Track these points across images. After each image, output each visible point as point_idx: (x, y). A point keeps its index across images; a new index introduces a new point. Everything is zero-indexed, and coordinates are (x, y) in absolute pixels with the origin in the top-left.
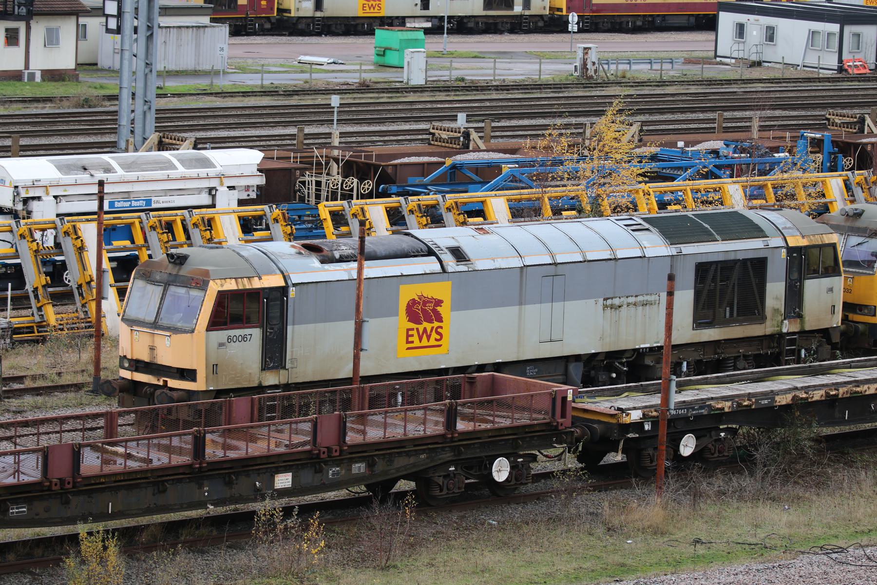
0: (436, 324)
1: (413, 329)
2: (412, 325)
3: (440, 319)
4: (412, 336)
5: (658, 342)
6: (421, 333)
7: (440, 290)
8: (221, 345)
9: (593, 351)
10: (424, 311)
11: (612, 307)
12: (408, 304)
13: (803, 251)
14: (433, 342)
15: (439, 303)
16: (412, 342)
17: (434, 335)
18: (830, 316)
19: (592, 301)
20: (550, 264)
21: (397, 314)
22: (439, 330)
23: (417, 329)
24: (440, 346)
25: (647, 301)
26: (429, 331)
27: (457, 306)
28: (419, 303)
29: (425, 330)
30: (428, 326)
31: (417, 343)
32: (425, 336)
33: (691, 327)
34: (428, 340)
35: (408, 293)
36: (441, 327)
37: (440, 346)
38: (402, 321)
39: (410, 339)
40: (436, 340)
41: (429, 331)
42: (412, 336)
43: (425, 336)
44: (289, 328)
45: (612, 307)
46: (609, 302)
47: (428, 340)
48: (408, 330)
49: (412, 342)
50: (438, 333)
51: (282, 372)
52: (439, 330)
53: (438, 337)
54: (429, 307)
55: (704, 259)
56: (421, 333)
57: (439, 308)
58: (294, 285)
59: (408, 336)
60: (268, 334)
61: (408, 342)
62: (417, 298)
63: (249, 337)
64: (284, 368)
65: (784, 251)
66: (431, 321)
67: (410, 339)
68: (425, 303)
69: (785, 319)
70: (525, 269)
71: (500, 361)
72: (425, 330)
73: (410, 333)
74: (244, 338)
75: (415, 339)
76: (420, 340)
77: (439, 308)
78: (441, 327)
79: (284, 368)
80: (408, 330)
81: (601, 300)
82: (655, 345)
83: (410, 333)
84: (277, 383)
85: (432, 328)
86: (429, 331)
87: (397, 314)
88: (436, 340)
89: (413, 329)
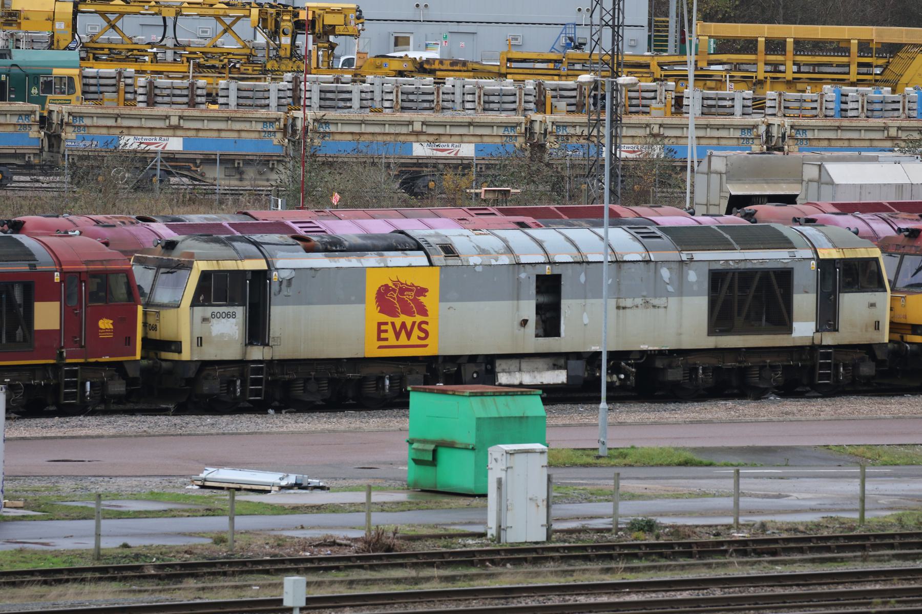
0: (419, 318)
1: (386, 324)
2: (384, 318)
3: (423, 311)
4: (386, 331)
6: (398, 330)
10: (400, 300)
12: (379, 292)
14: (414, 340)
15: (422, 291)
16: (386, 339)
17: (416, 332)
21: (362, 300)
22: (424, 326)
23: (393, 324)
24: (425, 346)
26: (409, 328)
27: (443, 298)
28: (394, 290)
29: (403, 325)
30: (409, 321)
31: (392, 341)
32: (403, 332)
34: (409, 338)
36: (426, 323)
37: (425, 346)
38: (371, 313)
39: (383, 335)
40: (419, 338)
41: (409, 328)
42: (386, 331)
43: (403, 332)
47: (409, 338)
48: (380, 324)
49: (386, 339)
52: (424, 326)
53: (423, 335)
54: (409, 296)
56: (398, 330)
57: (422, 299)
59: (380, 331)
61: (379, 339)
62: (391, 284)
65: (813, 264)
66: (410, 313)
67: (383, 335)
72: (403, 325)
73: (383, 327)
75: (391, 335)
77: (422, 299)
78: (426, 323)
80: (380, 324)
83: (383, 327)
85: (414, 323)
86: (409, 327)
88: (419, 338)
89: (386, 324)
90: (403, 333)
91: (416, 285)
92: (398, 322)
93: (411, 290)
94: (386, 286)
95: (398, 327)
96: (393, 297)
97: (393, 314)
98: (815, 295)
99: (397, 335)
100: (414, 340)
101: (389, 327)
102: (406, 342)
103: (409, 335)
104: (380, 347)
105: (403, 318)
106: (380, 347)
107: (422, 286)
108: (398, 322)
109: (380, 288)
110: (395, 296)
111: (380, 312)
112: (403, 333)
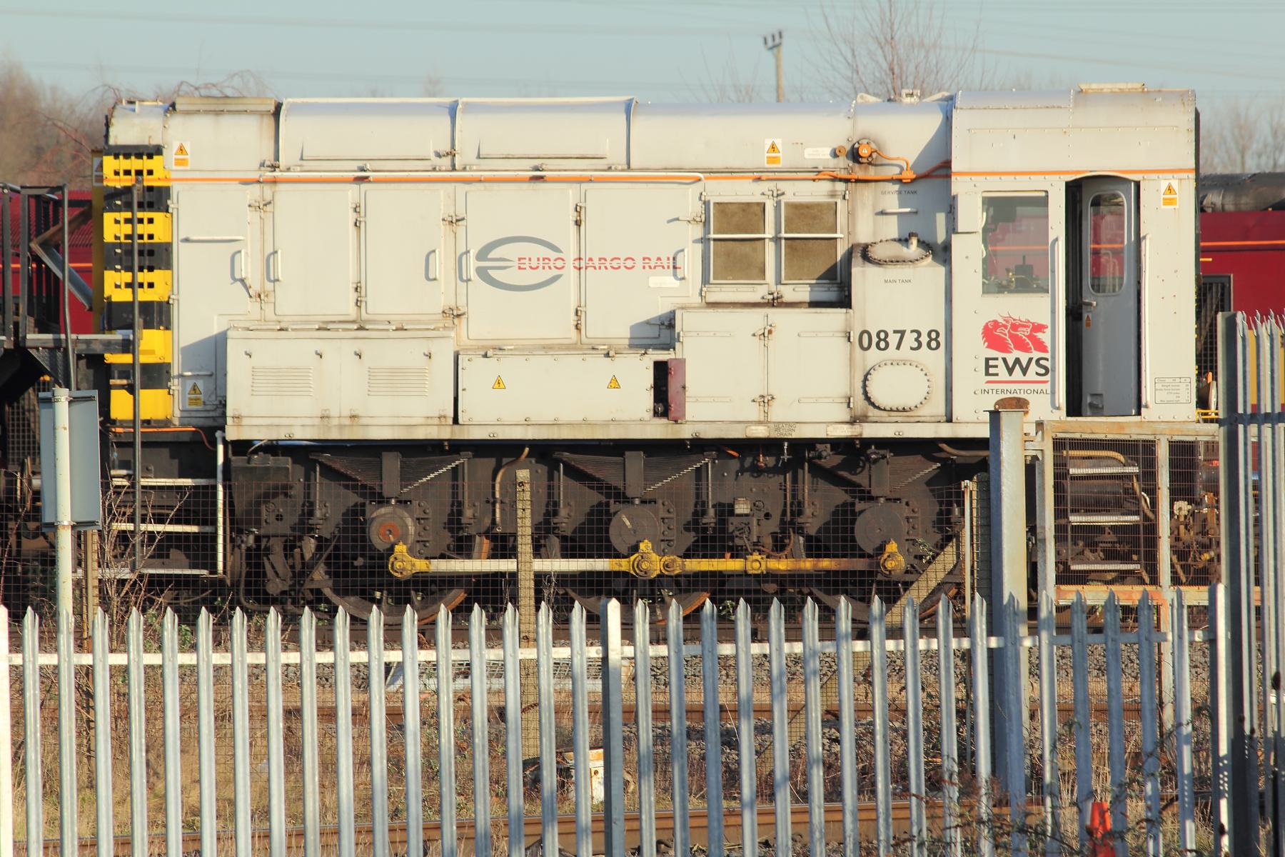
2: (993, 353)
23: (1005, 360)
28: (1006, 327)
29: (1017, 361)
30: (1024, 358)
39: (992, 370)
54: (1023, 333)
57: (1039, 335)
59: (987, 366)
61: (987, 374)
62: (1001, 320)
66: (1027, 350)
67: (992, 370)
68: (1015, 327)
72: (1017, 361)
73: (991, 363)
80: (987, 360)
83: (991, 363)
85: (1030, 360)
94: (996, 322)
96: (1004, 333)
97: (1004, 348)
99: (1010, 371)
102: (1022, 378)
103: (1024, 371)
104: (988, 382)
105: (1017, 354)
106: (988, 382)
107: (1039, 322)
110: (1006, 332)
111: (989, 347)
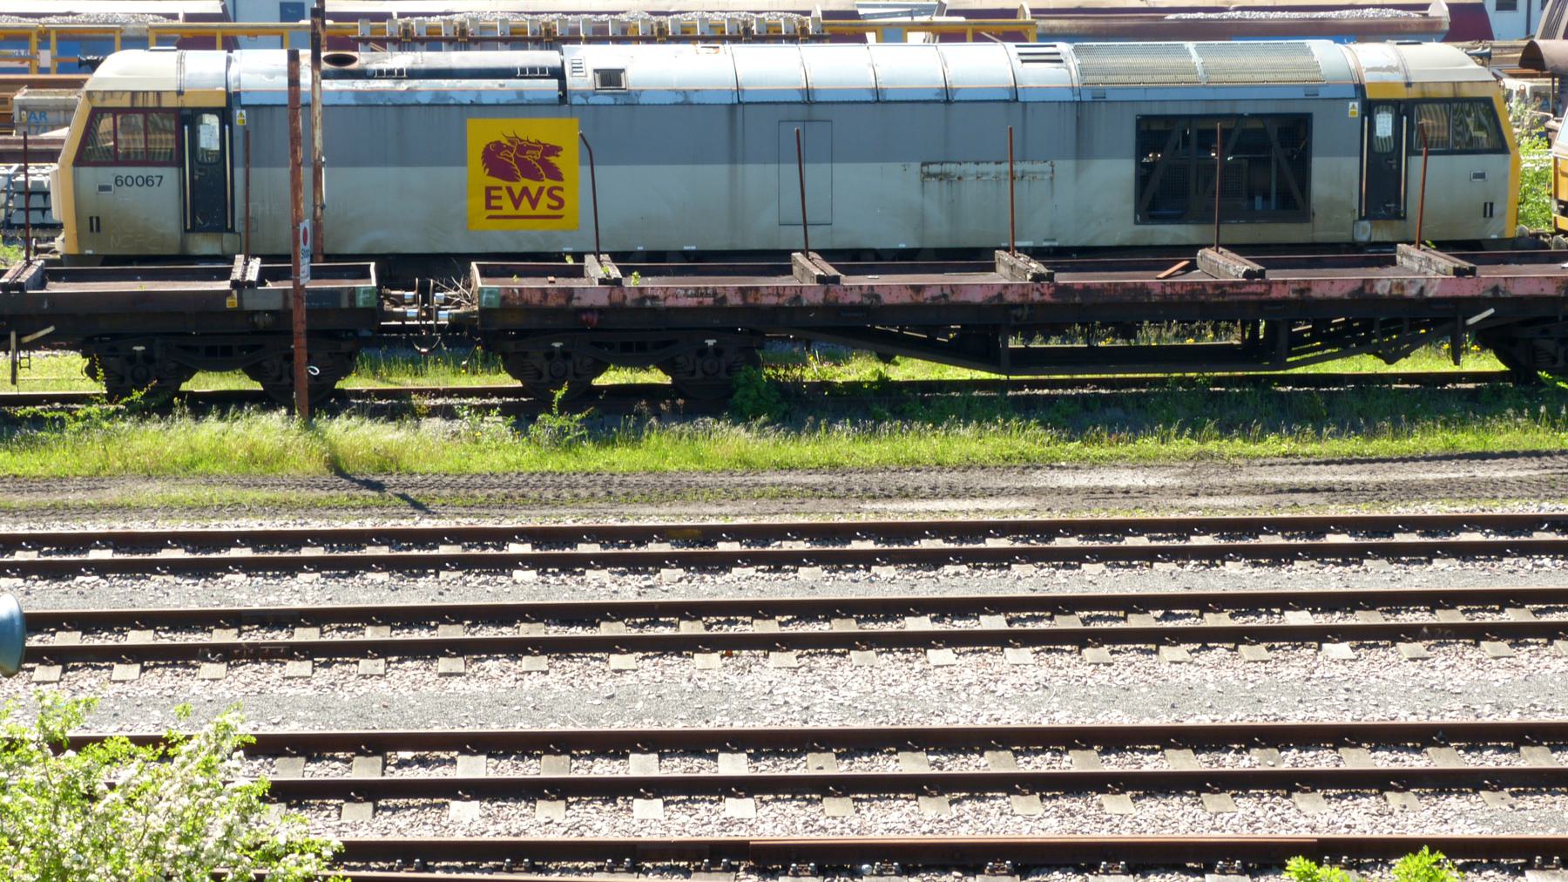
0: (548, 183)
1: (499, 188)
3: (555, 174)
4: (499, 198)
5: (1054, 240)
6: (517, 195)
7: (561, 132)
8: (103, 188)
9: (902, 246)
11: (941, 177)
13: (1402, 107)
15: (553, 150)
17: (545, 200)
18: (1482, 220)
19: (895, 167)
20: (799, 103)
21: (461, 161)
22: (555, 192)
23: (509, 190)
25: (1023, 171)
26: (534, 194)
28: (508, 148)
29: (525, 191)
30: (533, 186)
33: (1132, 220)
35: (482, 133)
36: (561, 189)
38: (476, 174)
39: (494, 203)
40: (550, 207)
42: (499, 198)
44: (239, 172)
45: (941, 177)
46: (934, 169)
48: (488, 190)
50: (550, 195)
51: (226, 236)
52: (556, 192)
53: (555, 203)
54: (532, 157)
55: (1156, 110)
56: (517, 195)
57: (552, 159)
58: (244, 107)
59: (489, 198)
60: (196, 177)
61: (489, 207)
62: (504, 141)
63: (157, 180)
64: (232, 230)
66: (538, 178)
67: (494, 203)
69: (1361, 218)
70: (740, 108)
71: (693, 248)
72: (525, 191)
73: (494, 193)
74: (147, 181)
76: (517, 204)
77: (552, 159)
78: (561, 189)
79: (232, 230)
80: (488, 190)
81: (916, 166)
82: (1046, 244)
83: (494, 193)
84: (217, 251)
85: (541, 190)
86: (534, 193)
87: (461, 161)
88: (550, 207)
89: (499, 188)
90: (525, 202)
91: (543, 141)
92: (517, 188)
93: (538, 149)
95: (517, 195)
98: (1358, 159)
99: (517, 204)
100: (542, 208)
101: (504, 193)
103: (534, 203)
104: (490, 217)
105: (525, 182)
106: (490, 217)
108: (517, 188)
109: (488, 146)
111: (489, 174)
112: (525, 202)
